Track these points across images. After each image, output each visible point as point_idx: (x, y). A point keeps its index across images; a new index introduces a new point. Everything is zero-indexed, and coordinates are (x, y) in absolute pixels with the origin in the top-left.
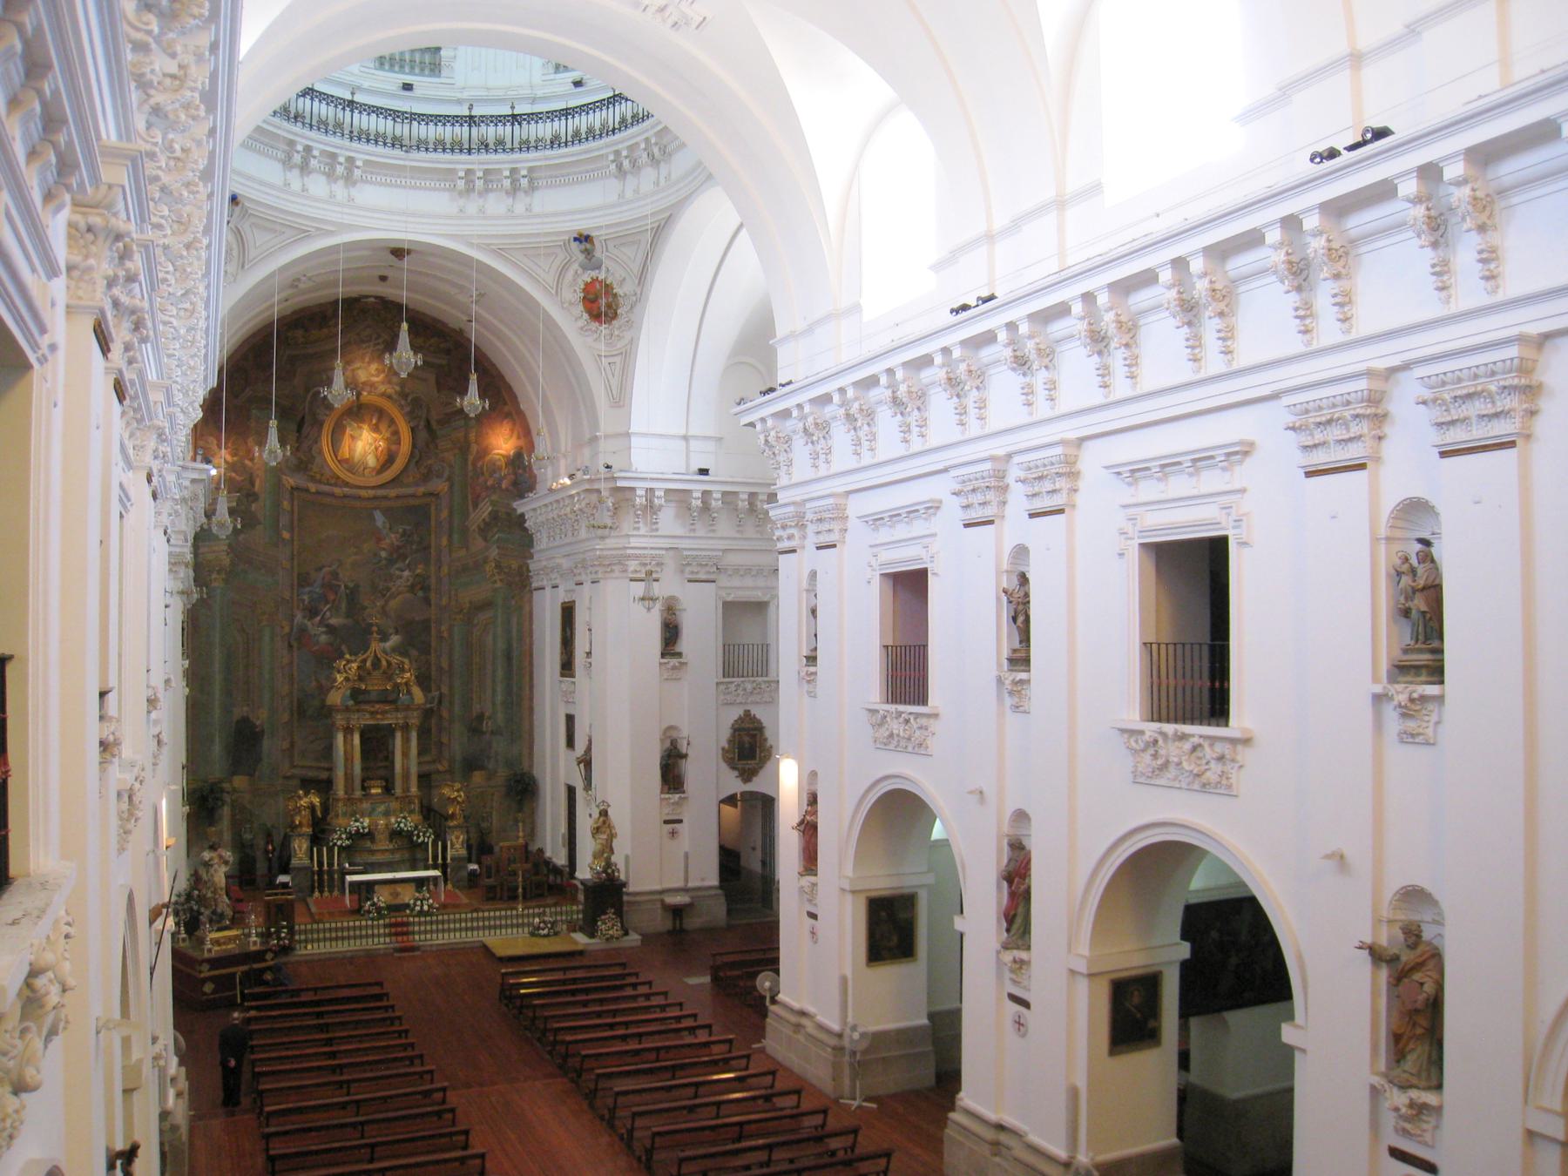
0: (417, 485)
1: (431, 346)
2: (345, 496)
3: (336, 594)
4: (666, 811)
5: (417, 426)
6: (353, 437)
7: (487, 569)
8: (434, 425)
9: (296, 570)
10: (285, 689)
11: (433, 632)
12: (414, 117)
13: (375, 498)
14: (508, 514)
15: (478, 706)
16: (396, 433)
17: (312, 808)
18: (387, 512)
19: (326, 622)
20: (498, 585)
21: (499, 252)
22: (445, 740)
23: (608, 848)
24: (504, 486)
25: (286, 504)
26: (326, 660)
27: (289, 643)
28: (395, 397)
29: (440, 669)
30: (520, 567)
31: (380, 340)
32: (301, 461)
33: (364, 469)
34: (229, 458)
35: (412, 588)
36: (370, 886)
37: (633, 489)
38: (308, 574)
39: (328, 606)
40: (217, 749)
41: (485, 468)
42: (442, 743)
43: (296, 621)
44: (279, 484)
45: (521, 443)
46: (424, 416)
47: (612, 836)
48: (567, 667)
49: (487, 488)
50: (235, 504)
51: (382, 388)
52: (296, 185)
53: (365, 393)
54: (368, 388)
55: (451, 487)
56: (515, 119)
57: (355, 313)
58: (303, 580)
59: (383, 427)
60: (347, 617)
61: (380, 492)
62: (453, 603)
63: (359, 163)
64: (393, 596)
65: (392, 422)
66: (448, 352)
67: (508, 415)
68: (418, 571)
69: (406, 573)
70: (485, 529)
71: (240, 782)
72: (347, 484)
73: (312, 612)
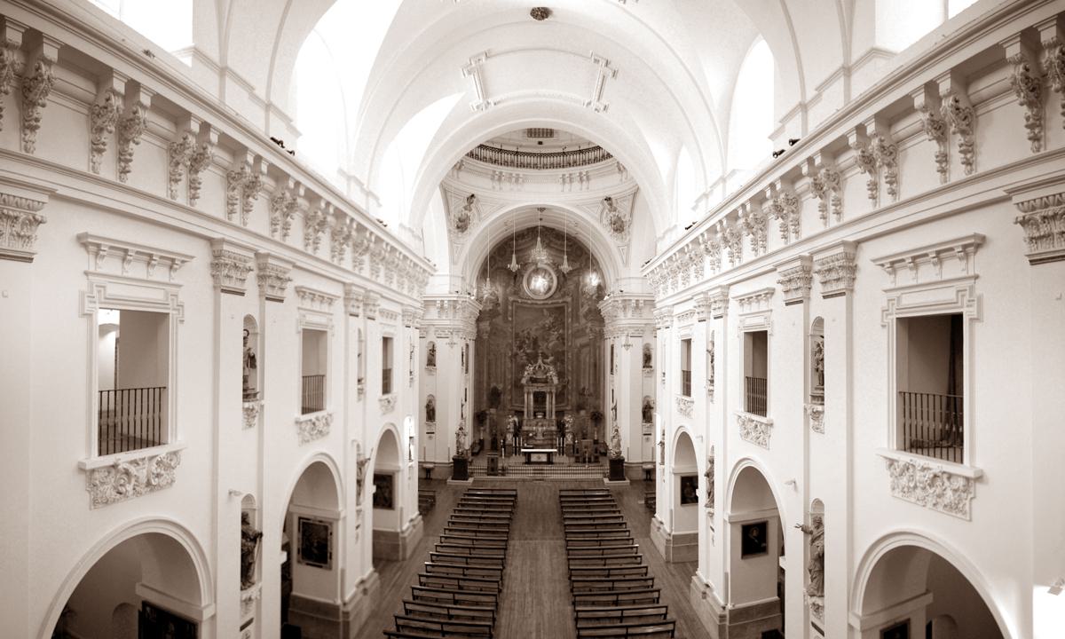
0: (559, 298)
2: (532, 304)
4: (645, 429)
6: (535, 281)
10: (510, 377)
12: (541, 155)
13: (544, 304)
16: (552, 279)
17: (514, 422)
18: (548, 309)
21: (577, 206)
22: (570, 397)
23: (619, 445)
25: (510, 308)
26: (523, 367)
29: (568, 370)
35: (557, 339)
36: (530, 453)
37: (630, 300)
40: (485, 398)
44: (507, 299)
45: (600, 281)
47: (619, 441)
48: (612, 374)
51: (545, 262)
52: (497, 187)
56: (581, 152)
59: (547, 276)
61: (546, 302)
63: (521, 176)
65: (550, 274)
67: (595, 270)
71: (493, 411)
73: (520, 347)
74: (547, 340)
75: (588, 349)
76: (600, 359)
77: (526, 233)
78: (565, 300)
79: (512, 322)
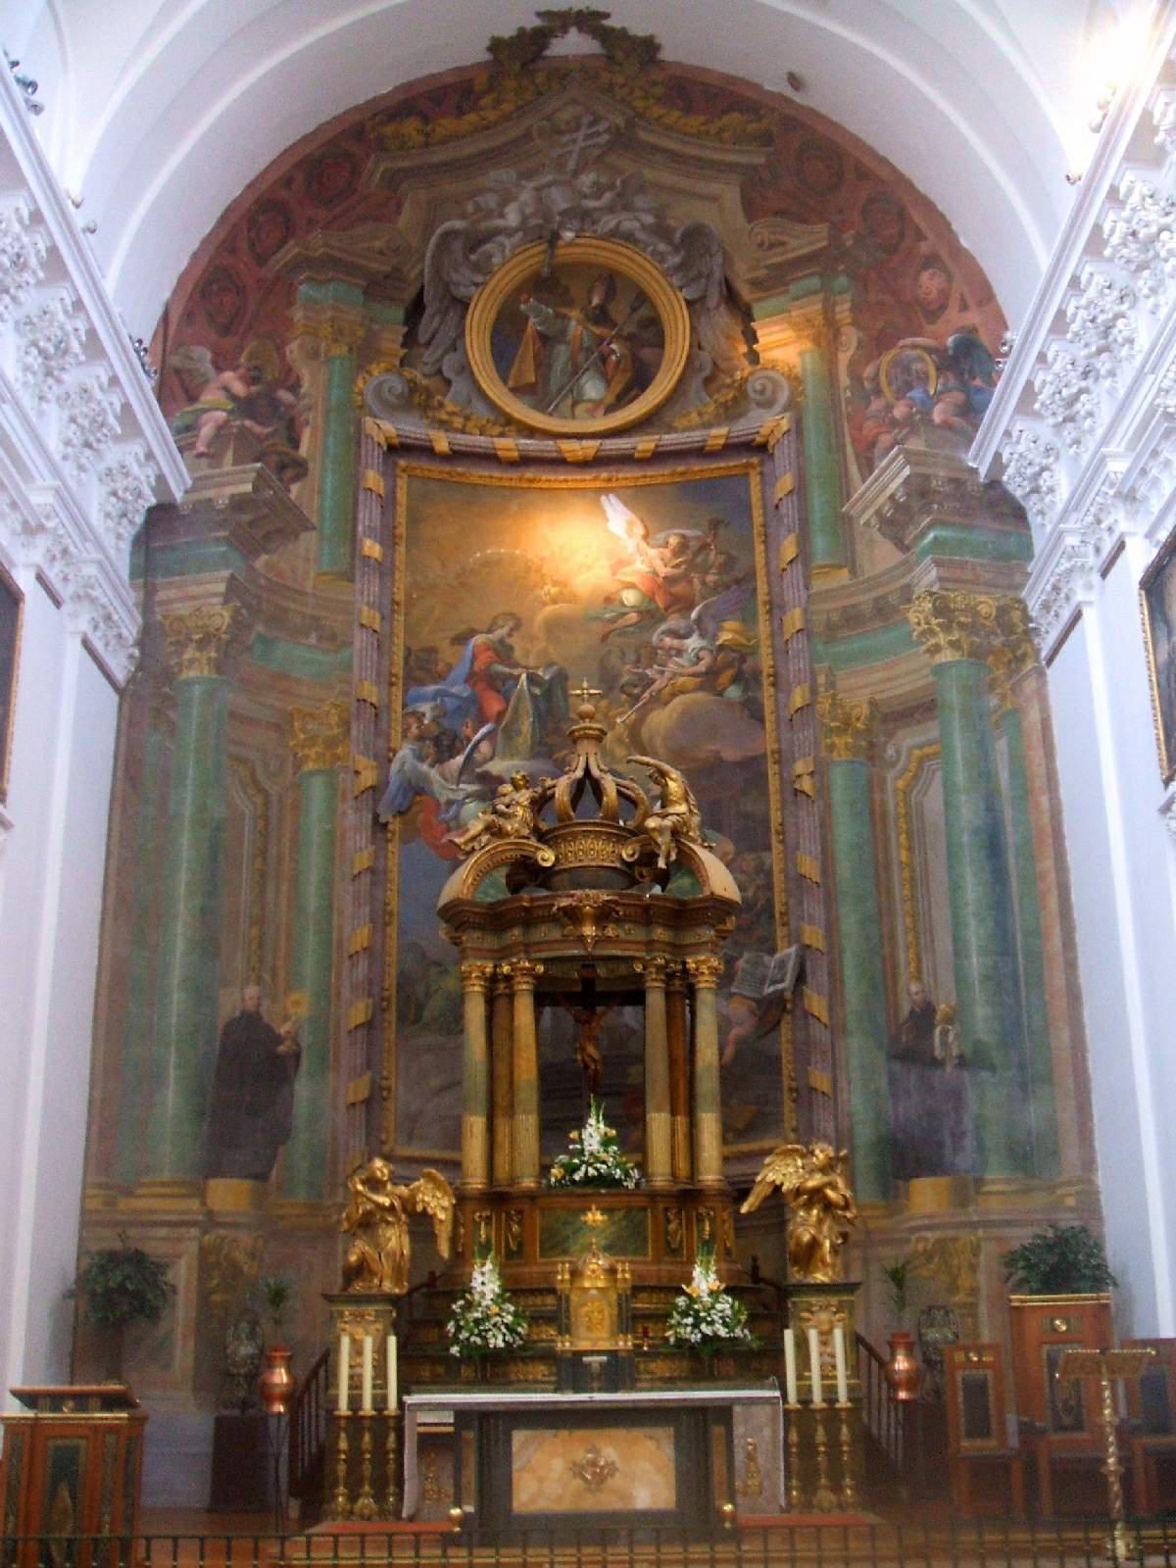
0: (708, 425)
1: (721, 130)
2: (526, 461)
3: (507, 700)
5: (703, 299)
7: (913, 617)
8: (745, 292)
9: (400, 642)
10: (361, 937)
11: (773, 783)
14: (957, 482)
15: (914, 988)
19: (478, 770)
20: (947, 656)
22: (821, 1080)
24: (937, 416)
27: (376, 817)
28: (641, 236)
30: (1003, 611)
31: (601, 127)
32: (413, 387)
33: (575, 404)
34: (239, 388)
35: (709, 680)
38: (432, 651)
39: (484, 730)
40: (171, 1100)
41: (883, 379)
42: (813, 1090)
43: (395, 767)
44: (357, 437)
46: (718, 274)
49: (894, 423)
50: (248, 488)
53: (569, 235)
54: (576, 224)
55: (798, 429)
57: (540, 78)
58: (421, 667)
60: (534, 755)
62: (824, 705)
64: (659, 701)
66: (766, 139)
68: (725, 637)
69: (693, 643)
70: (896, 524)
71: (228, 1194)
72: (531, 432)
73: (443, 744)
74: (636, 692)
75: (933, 730)
76: (1024, 793)
77: (481, 82)
78: (741, 428)
79: (385, 570)
